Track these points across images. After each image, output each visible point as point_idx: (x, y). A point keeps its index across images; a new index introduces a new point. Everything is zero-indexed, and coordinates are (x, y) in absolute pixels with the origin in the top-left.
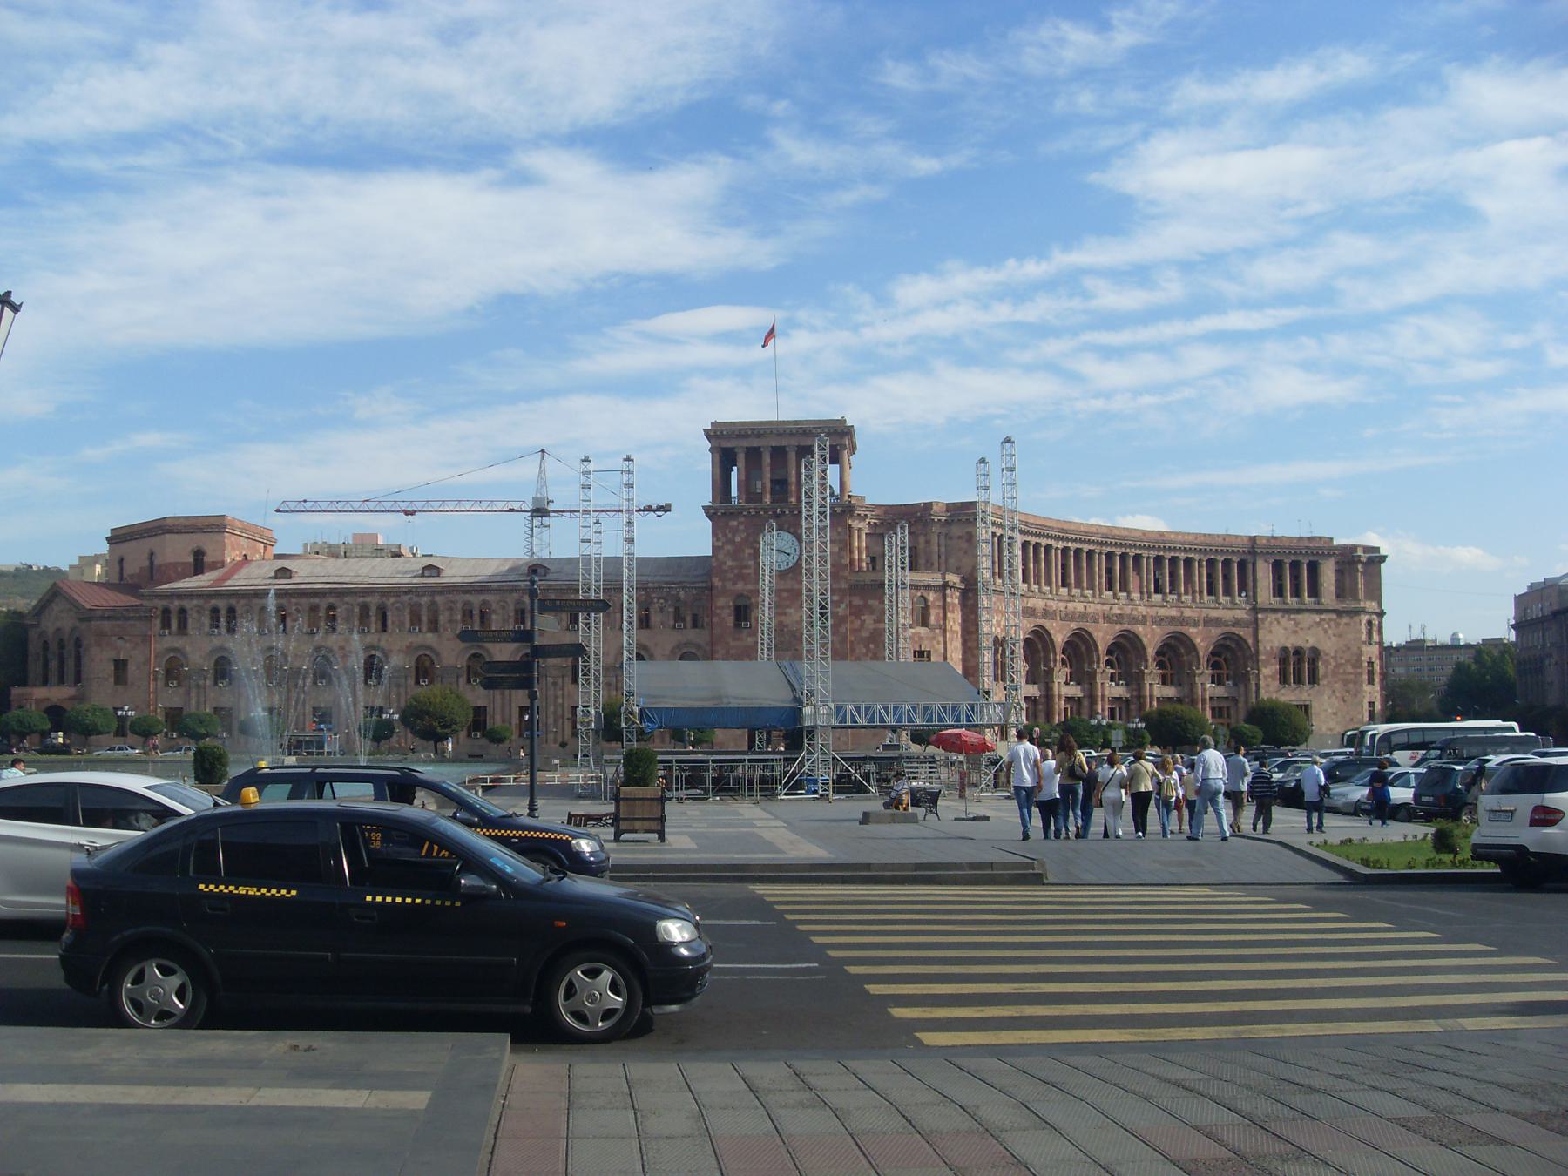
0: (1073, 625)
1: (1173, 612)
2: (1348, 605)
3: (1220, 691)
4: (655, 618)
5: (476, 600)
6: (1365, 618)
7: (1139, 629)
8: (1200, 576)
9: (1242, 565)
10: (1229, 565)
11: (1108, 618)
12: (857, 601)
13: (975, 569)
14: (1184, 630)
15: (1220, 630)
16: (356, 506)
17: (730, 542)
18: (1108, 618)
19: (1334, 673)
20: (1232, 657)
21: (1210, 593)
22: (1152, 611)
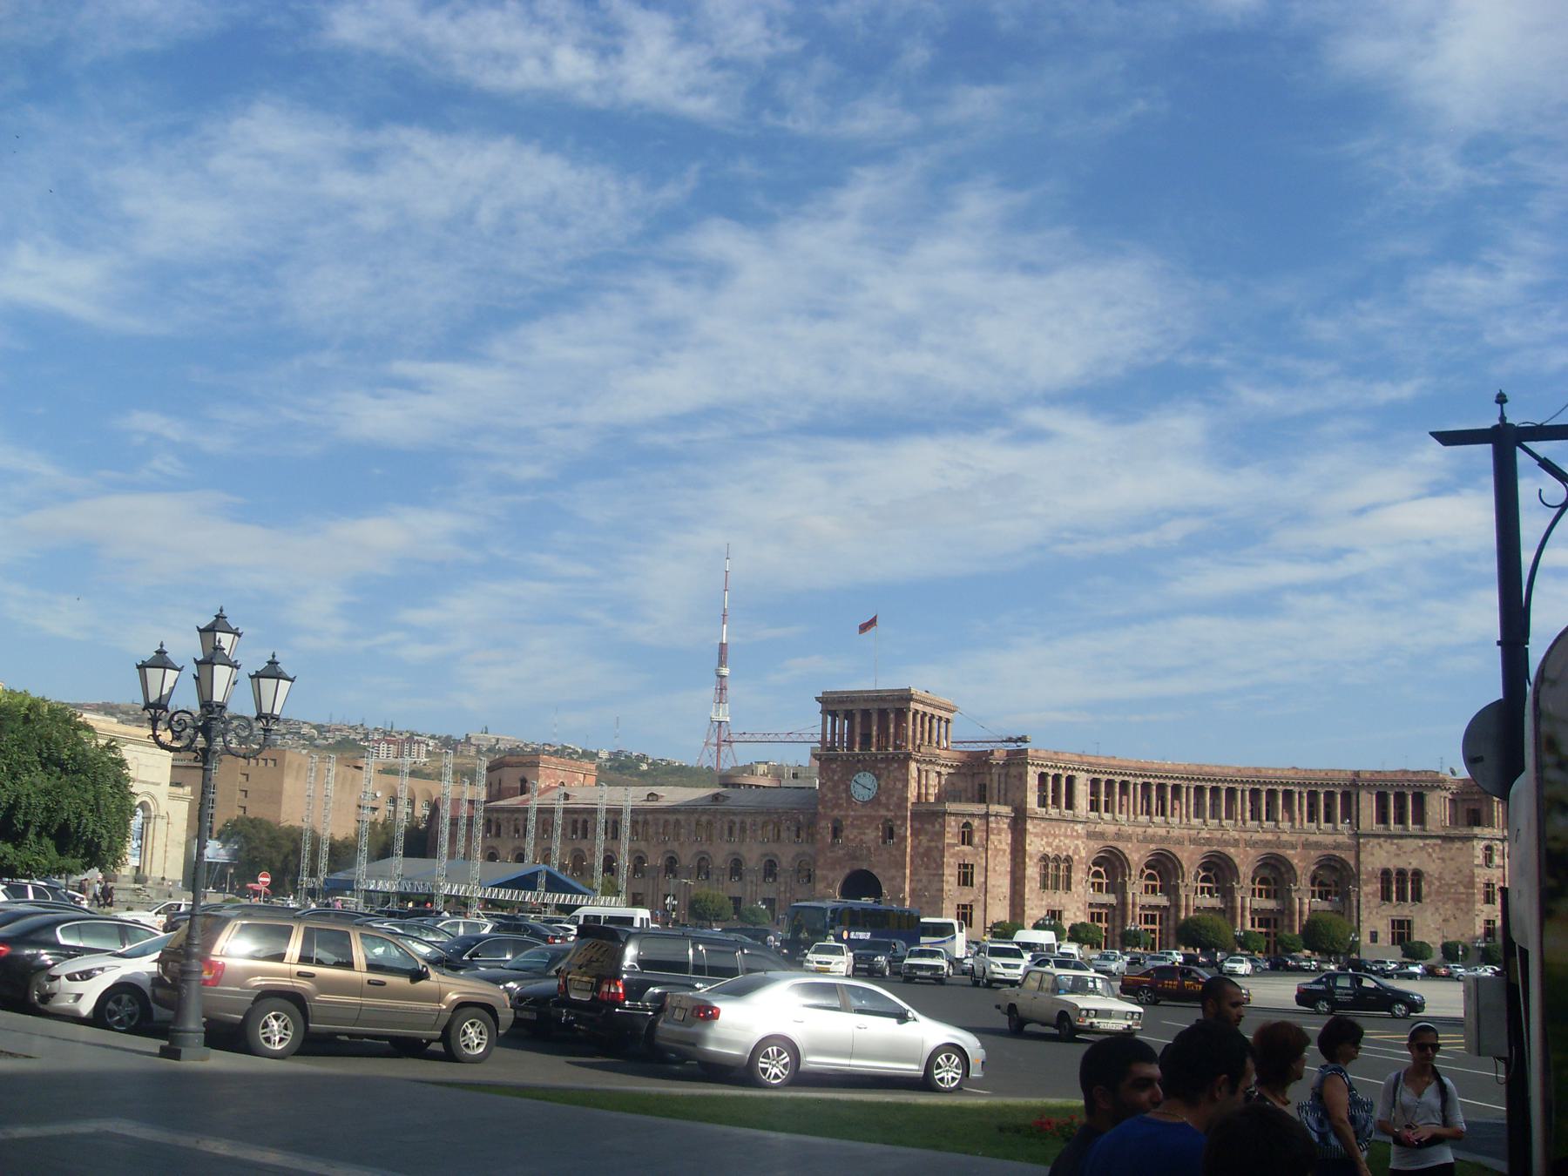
0: (1152, 846)
1: (1269, 837)
2: (1464, 831)
3: (1319, 904)
4: (784, 835)
5: (671, 818)
6: (1479, 846)
7: (1231, 851)
8: (1301, 806)
9: (1346, 796)
10: (1334, 797)
11: (1193, 841)
12: (917, 825)
13: (1024, 801)
14: (1281, 852)
15: (1319, 853)
16: (782, 737)
17: (831, 779)
18: (1193, 841)
19: (1438, 893)
20: (1336, 877)
21: (1311, 820)
22: (1246, 836)
